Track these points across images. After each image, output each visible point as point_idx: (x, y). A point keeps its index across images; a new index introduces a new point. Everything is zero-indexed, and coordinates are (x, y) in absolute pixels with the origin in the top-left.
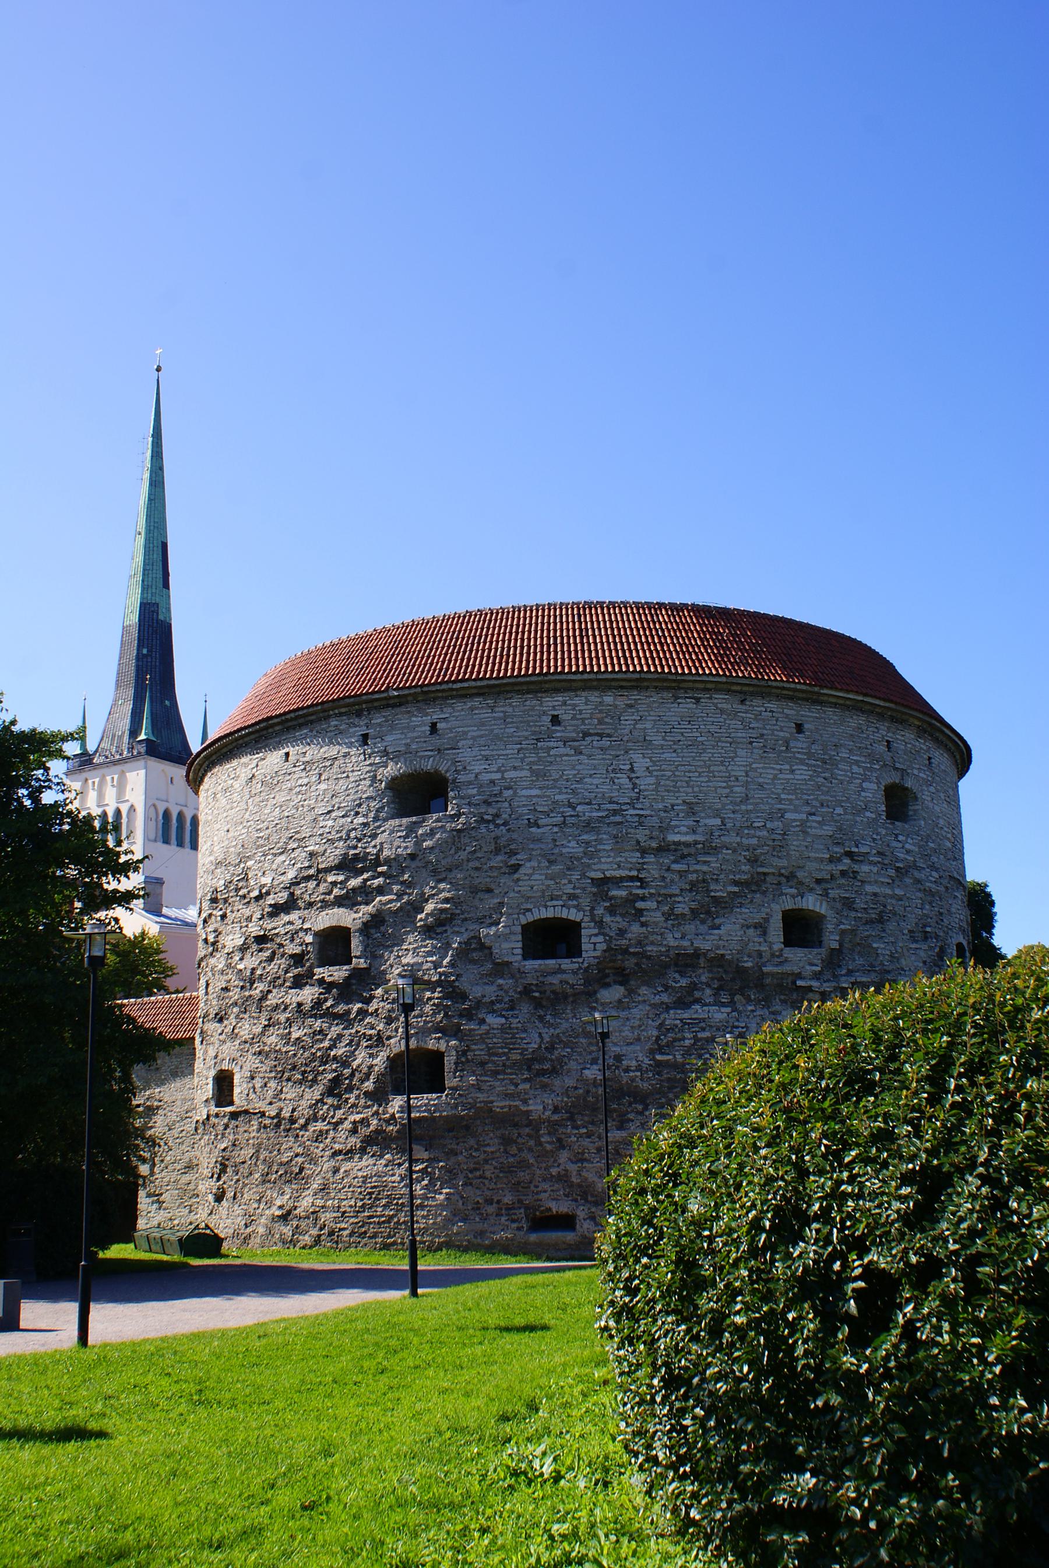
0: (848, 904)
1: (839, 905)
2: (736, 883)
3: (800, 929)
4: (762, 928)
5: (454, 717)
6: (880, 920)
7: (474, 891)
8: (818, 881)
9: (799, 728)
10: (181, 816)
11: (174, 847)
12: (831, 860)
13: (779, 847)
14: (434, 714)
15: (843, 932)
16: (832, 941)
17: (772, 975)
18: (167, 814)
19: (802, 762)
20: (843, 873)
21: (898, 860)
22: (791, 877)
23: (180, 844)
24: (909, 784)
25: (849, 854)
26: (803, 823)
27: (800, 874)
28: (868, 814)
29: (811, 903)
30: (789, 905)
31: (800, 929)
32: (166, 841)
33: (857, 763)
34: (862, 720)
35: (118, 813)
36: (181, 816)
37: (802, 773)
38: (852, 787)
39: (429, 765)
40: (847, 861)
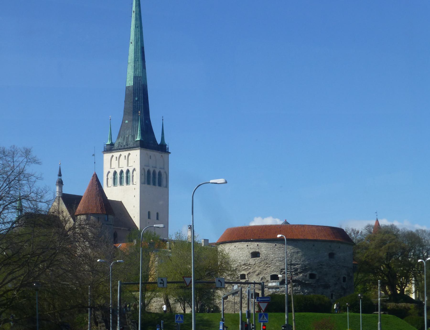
5: (260, 244)
7: (263, 270)
9: (314, 246)
10: (154, 172)
11: (152, 185)
14: (258, 243)
16: (317, 278)
18: (149, 172)
23: (154, 184)
25: (321, 265)
29: (314, 272)
32: (149, 183)
35: (128, 171)
36: (154, 172)
39: (257, 251)
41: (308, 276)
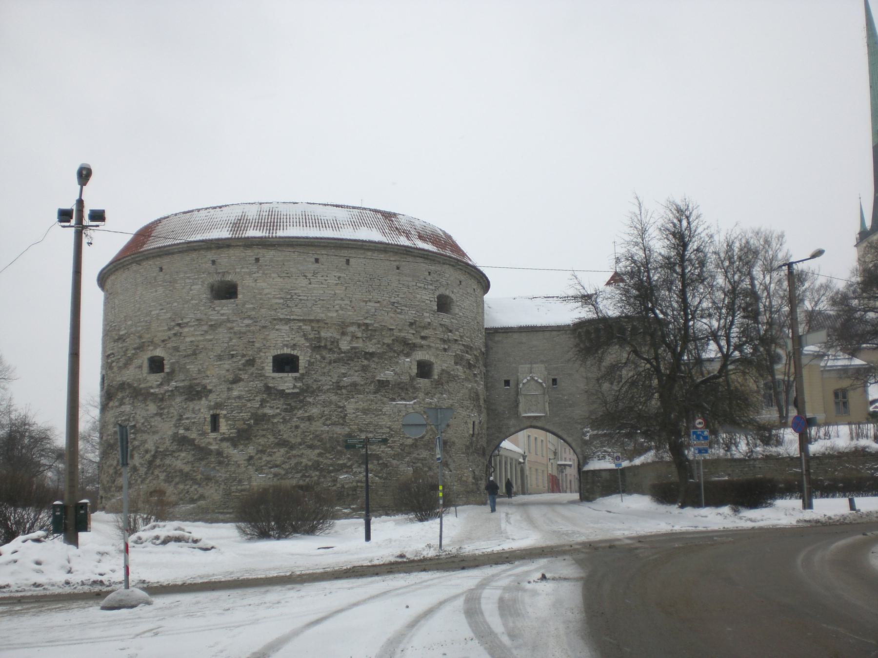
0: (176, 349)
1: (171, 351)
2: (135, 349)
3: (156, 365)
4: (140, 367)
6: (194, 354)
8: (163, 341)
9: (161, 269)
12: (170, 329)
13: (148, 329)
15: (173, 364)
16: (167, 369)
17: (144, 388)
19: (161, 285)
20: (175, 335)
21: (211, 320)
22: (152, 342)
24: (229, 278)
25: (179, 325)
26: (158, 315)
27: (155, 339)
28: (194, 302)
29: (159, 352)
30: (150, 354)
31: (156, 365)
33: (189, 278)
34: (194, 255)
37: (160, 290)
38: (184, 290)
40: (177, 328)
41: (146, 365)
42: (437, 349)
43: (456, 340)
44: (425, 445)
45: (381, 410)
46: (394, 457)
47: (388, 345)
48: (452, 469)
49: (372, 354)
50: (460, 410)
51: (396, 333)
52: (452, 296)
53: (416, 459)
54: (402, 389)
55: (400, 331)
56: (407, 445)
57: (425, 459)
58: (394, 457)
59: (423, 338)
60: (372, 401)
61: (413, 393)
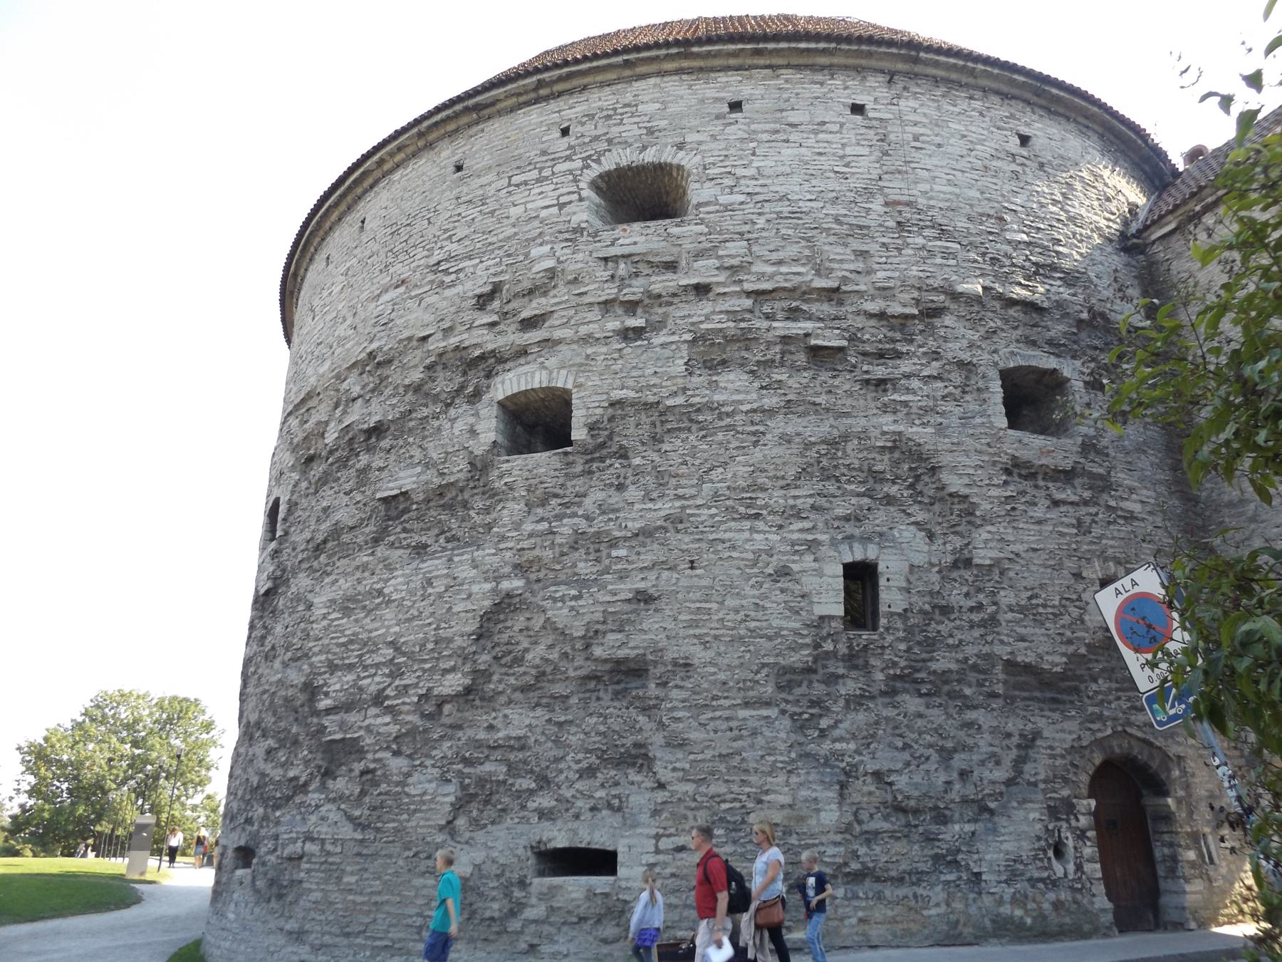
42: (587, 340)
43: (702, 290)
44: (524, 689)
45: (380, 592)
46: (396, 745)
47: (417, 388)
48: (664, 774)
49: (377, 431)
50: (737, 532)
51: (436, 345)
52: (682, 158)
53: (478, 744)
54: (449, 507)
55: (448, 331)
56: (442, 701)
57: (521, 744)
58: (396, 745)
59: (529, 324)
60: (364, 567)
61: (487, 510)
